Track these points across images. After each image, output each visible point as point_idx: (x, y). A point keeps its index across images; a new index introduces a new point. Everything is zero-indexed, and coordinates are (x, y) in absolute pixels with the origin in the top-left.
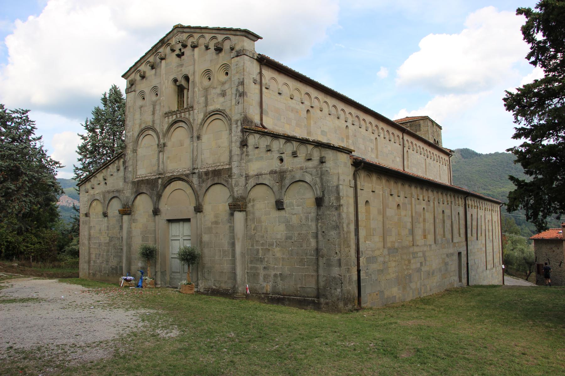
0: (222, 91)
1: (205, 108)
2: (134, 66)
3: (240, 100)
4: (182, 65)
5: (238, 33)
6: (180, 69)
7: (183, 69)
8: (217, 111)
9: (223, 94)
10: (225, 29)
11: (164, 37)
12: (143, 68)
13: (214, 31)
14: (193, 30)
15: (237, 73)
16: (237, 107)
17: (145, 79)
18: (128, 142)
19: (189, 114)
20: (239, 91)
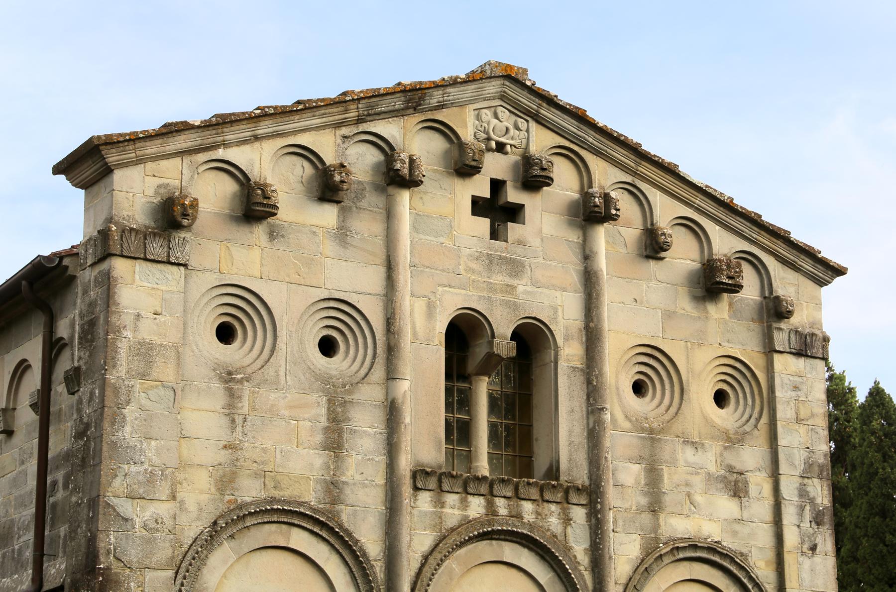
0: (731, 469)
1: (646, 518)
2: (207, 126)
3: (819, 540)
4: (515, 267)
5: (807, 265)
6: (500, 278)
7: (522, 286)
8: (711, 550)
9: (737, 488)
10: (754, 221)
11: (436, 86)
12: (261, 160)
13: (699, 201)
14: (591, 138)
15: (798, 420)
16: (807, 563)
17: (260, 231)
18: (133, 554)
19: (567, 521)
20: (812, 501)
